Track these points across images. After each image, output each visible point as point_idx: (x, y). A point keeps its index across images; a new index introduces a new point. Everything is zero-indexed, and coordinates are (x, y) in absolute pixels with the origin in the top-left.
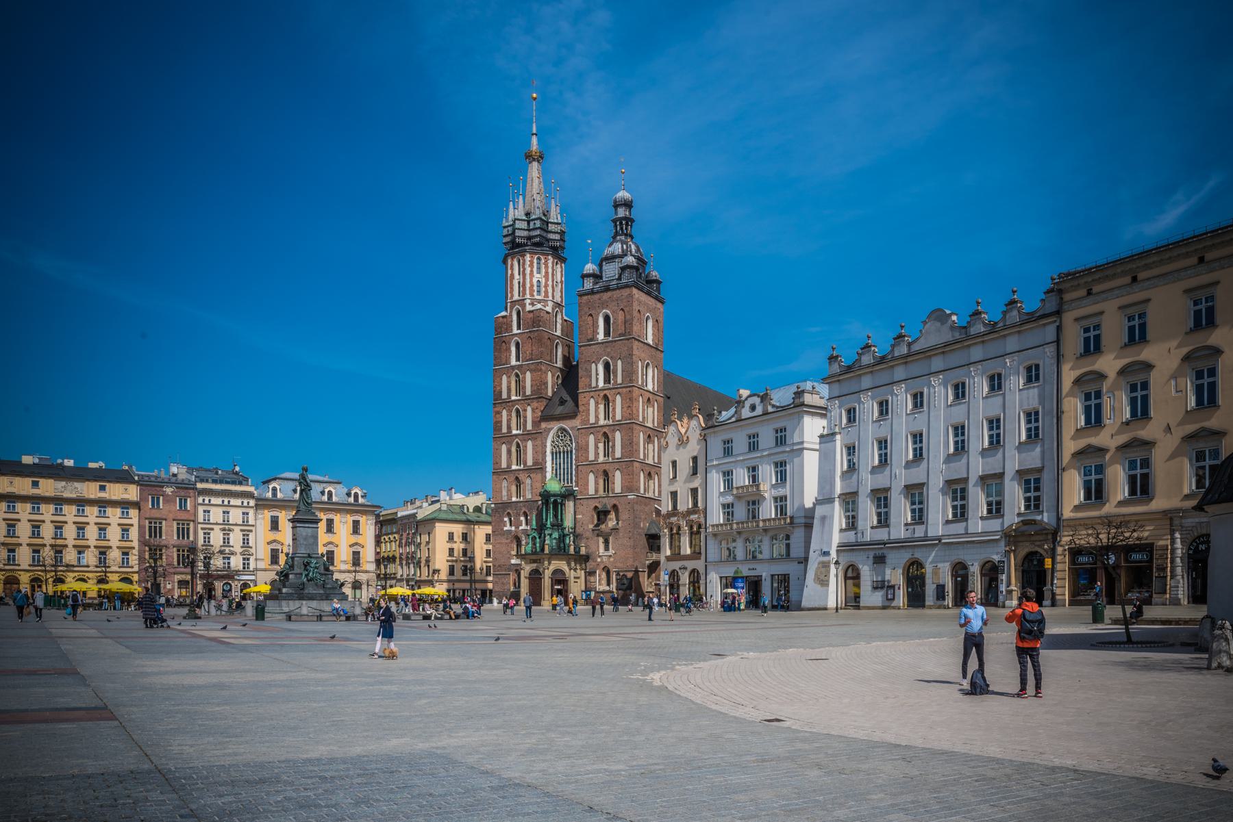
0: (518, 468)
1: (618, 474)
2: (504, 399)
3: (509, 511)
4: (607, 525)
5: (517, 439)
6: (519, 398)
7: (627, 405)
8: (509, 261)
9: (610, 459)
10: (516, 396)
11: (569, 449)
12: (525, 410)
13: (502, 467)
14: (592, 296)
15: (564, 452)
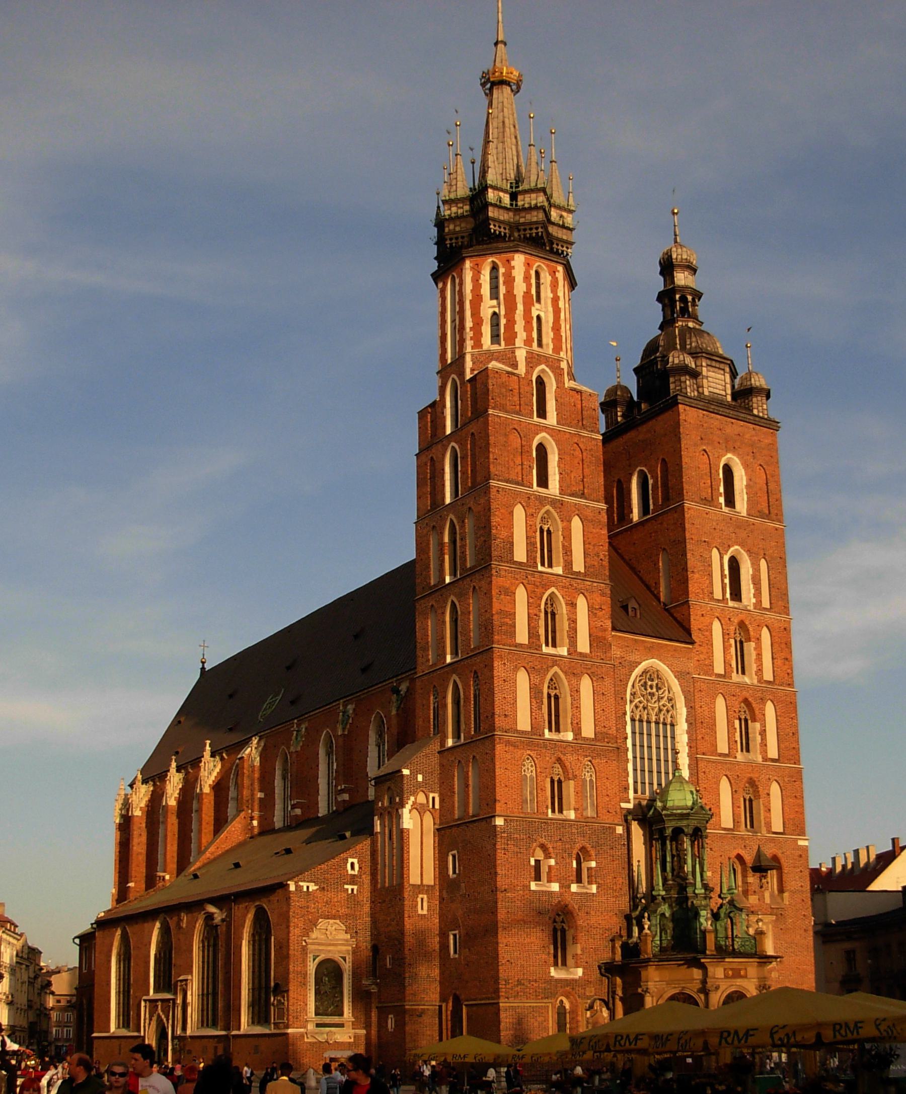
0: (554, 736)
1: (775, 789)
2: (520, 563)
3: (543, 840)
4: (761, 899)
5: (556, 669)
6: (549, 570)
7: (783, 655)
8: (519, 260)
9: (760, 759)
10: (543, 564)
11: (669, 721)
12: (572, 605)
13: (520, 727)
14: (706, 418)
15: (657, 723)
